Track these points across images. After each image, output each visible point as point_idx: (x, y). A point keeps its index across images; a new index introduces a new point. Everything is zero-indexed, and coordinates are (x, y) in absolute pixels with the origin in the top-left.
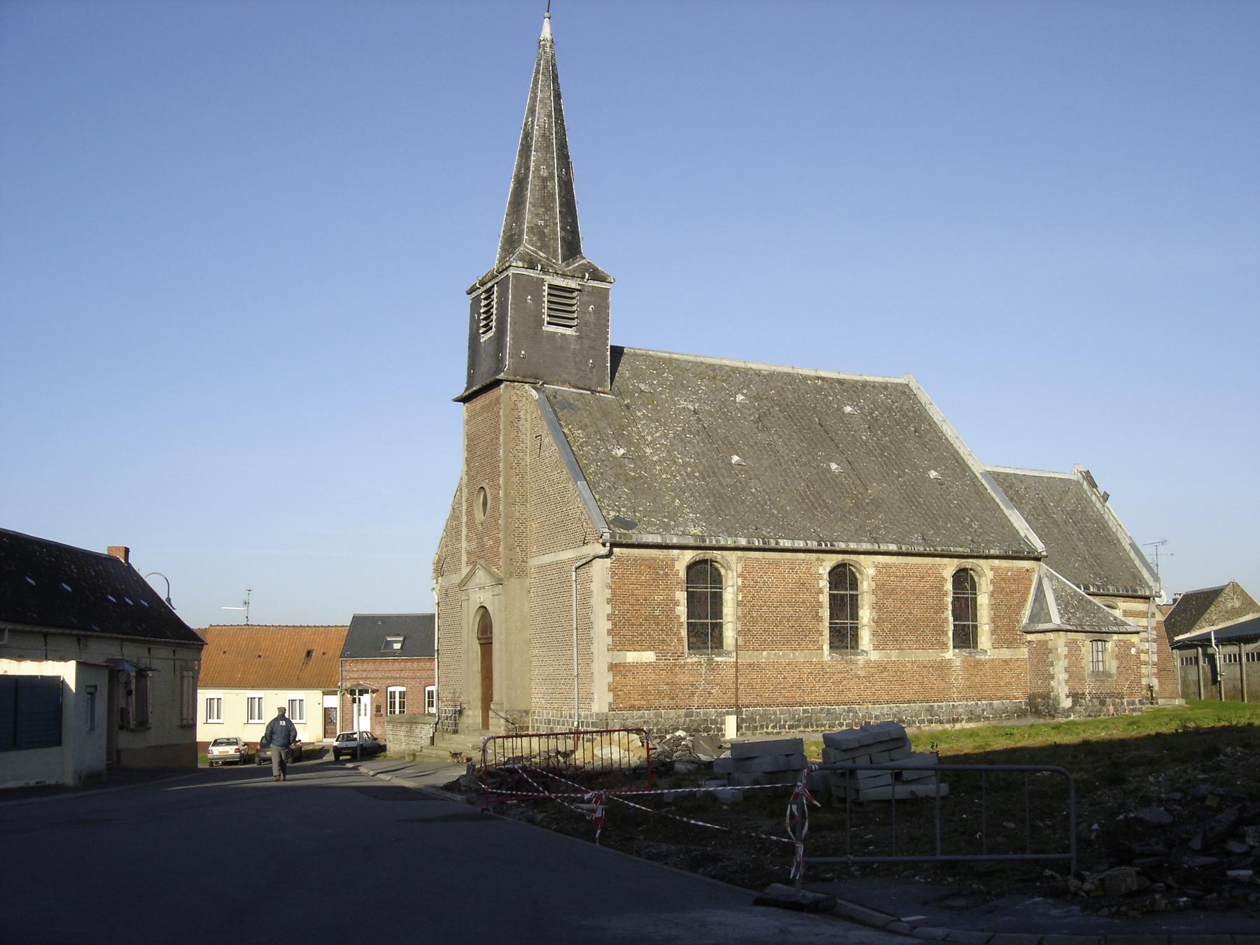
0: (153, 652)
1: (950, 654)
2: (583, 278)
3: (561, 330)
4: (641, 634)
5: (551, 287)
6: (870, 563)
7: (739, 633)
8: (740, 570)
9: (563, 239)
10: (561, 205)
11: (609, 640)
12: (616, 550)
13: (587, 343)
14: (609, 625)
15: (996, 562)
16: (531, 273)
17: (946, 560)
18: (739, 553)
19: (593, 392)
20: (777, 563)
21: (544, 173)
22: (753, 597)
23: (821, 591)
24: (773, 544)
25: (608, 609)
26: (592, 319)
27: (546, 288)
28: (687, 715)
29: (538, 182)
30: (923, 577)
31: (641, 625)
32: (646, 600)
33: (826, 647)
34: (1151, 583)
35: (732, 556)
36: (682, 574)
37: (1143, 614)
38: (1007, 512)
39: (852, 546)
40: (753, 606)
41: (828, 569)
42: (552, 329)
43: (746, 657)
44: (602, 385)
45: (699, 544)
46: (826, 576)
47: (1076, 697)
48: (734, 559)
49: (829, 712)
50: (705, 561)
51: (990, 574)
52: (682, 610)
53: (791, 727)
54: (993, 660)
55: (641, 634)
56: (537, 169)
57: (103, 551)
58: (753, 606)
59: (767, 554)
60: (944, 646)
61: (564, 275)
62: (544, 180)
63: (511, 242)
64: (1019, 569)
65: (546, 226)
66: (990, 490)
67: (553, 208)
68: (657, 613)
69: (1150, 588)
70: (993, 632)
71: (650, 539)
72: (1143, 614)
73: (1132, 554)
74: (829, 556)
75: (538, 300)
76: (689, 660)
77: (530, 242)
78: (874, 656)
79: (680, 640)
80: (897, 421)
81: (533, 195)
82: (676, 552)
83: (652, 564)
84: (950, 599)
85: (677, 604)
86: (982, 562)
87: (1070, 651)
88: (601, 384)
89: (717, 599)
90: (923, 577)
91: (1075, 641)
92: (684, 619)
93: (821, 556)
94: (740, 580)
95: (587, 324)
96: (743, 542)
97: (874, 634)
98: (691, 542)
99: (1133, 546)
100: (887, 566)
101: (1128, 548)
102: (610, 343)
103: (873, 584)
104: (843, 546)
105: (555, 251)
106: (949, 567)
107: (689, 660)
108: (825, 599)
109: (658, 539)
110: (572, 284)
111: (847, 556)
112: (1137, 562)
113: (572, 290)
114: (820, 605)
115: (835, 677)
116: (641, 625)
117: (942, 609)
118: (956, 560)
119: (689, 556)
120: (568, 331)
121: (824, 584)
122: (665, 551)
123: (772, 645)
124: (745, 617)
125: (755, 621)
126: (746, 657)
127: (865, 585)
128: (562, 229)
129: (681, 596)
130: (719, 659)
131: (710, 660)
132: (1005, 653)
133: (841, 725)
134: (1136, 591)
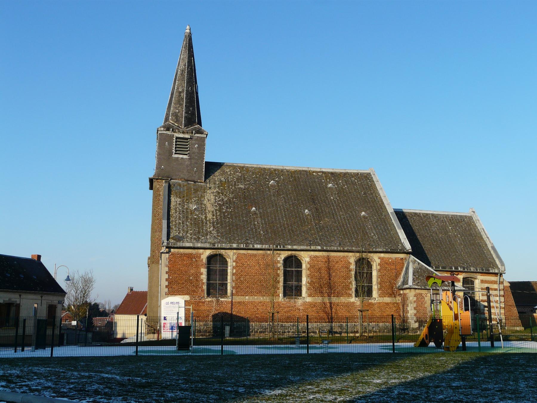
0: (43, 298)
1: (353, 299)
2: (192, 133)
3: (181, 156)
4: (183, 287)
5: (177, 138)
6: (307, 256)
7: (233, 288)
8: (234, 259)
9: (186, 117)
10: (186, 103)
11: (167, 290)
12: (172, 250)
13: (193, 161)
14: (167, 283)
15: (382, 255)
16: (168, 132)
17: (351, 254)
18: (235, 251)
19: (195, 182)
20: (255, 255)
21: (180, 90)
22: (242, 271)
23: (279, 269)
24: (251, 246)
25: (167, 276)
26: (196, 151)
27: (175, 139)
28: (205, 325)
29: (177, 94)
30: (337, 262)
31: (183, 283)
32: (186, 272)
33: (281, 295)
34: (500, 266)
35: (231, 253)
36: (205, 260)
37: (495, 282)
38: (398, 231)
39: (295, 247)
40: (242, 275)
41: (283, 258)
42: (176, 156)
43: (237, 299)
44: (201, 179)
45: (211, 246)
46: (282, 262)
47: (421, 323)
48: (232, 254)
49: (282, 326)
50: (216, 255)
51: (378, 261)
52: (204, 277)
53: (261, 332)
54: (379, 303)
55: (183, 287)
56: (178, 88)
57: (29, 257)
58: (242, 275)
59: (249, 252)
60: (350, 295)
61: (183, 133)
62: (180, 92)
63: (167, 119)
64: (396, 258)
65: (179, 112)
66: (393, 221)
67: (182, 104)
68: (191, 278)
69: (498, 268)
70: (379, 289)
71: (188, 245)
72: (495, 282)
73: (492, 252)
74: (282, 252)
75: (171, 144)
76: (207, 300)
77: (172, 119)
78: (309, 300)
79: (203, 291)
80: (361, 188)
81: (175, 100)
82: (201, 251)
83: (190, 256)
84: (353, 273)
85: (202, 274)
86: (372, 255)
87: (417, 299)
88: (200, 178)
89: (224, 273)
90: (337, 262)
91: (421, 294)
92: (205, 281)
93: (278, 252)
94: (234, 264)
95: (194, 153)
96: (235, 246)
97: (308, 289)
98: (208, 245)
99: (493, 248)
100: (316, 257)
101: (490, 249)
102: (205, 160)
103: (309, 266)
104: (290, 247)
105: (182, 122)
106: (352, 258)
107: (207, 300)
108: (281, 272)
109: (191, 245)
110: (187, 136)
111: (294, 252)
112: (494, 256)
113: (187, 139)
114: (278, 275)
115: (286, 309)
116: (183, 283)
117: (349, 277)
118: (287, 252)
119: (208, 252)
120: (185, 157)
121: (280, 265)
122: (196, 250)
123: (251, 294)
124: (237, 280)
125: (242, 282)
126: (237, 299)
127: (231, 264)
128: (186, 113)
129: (204, 271)
130: (223, 299)
131: (218, 301)
132: (387, 300)
133: (289, 332)
134: (489, 270)
